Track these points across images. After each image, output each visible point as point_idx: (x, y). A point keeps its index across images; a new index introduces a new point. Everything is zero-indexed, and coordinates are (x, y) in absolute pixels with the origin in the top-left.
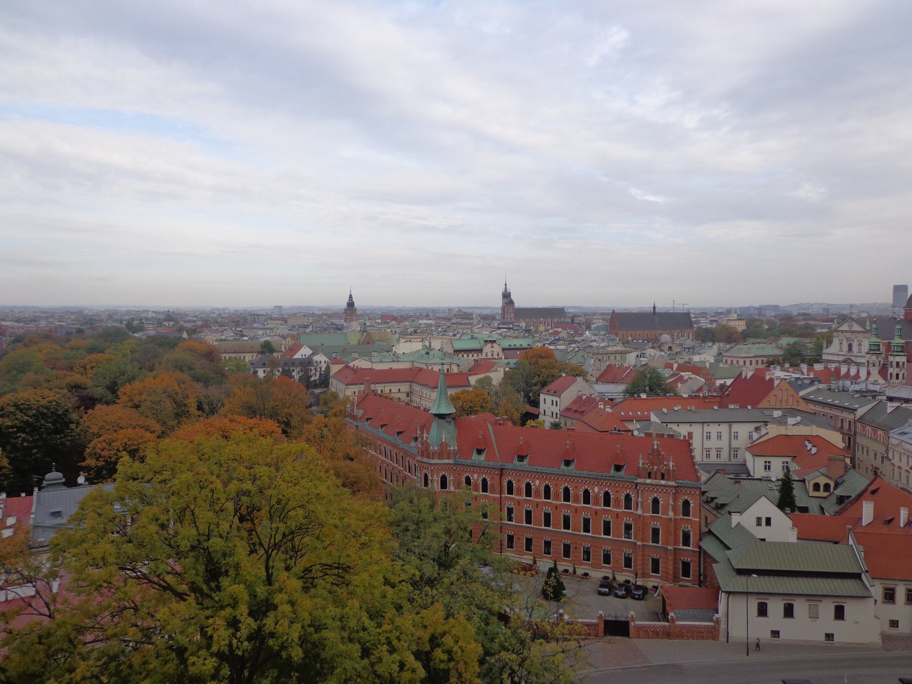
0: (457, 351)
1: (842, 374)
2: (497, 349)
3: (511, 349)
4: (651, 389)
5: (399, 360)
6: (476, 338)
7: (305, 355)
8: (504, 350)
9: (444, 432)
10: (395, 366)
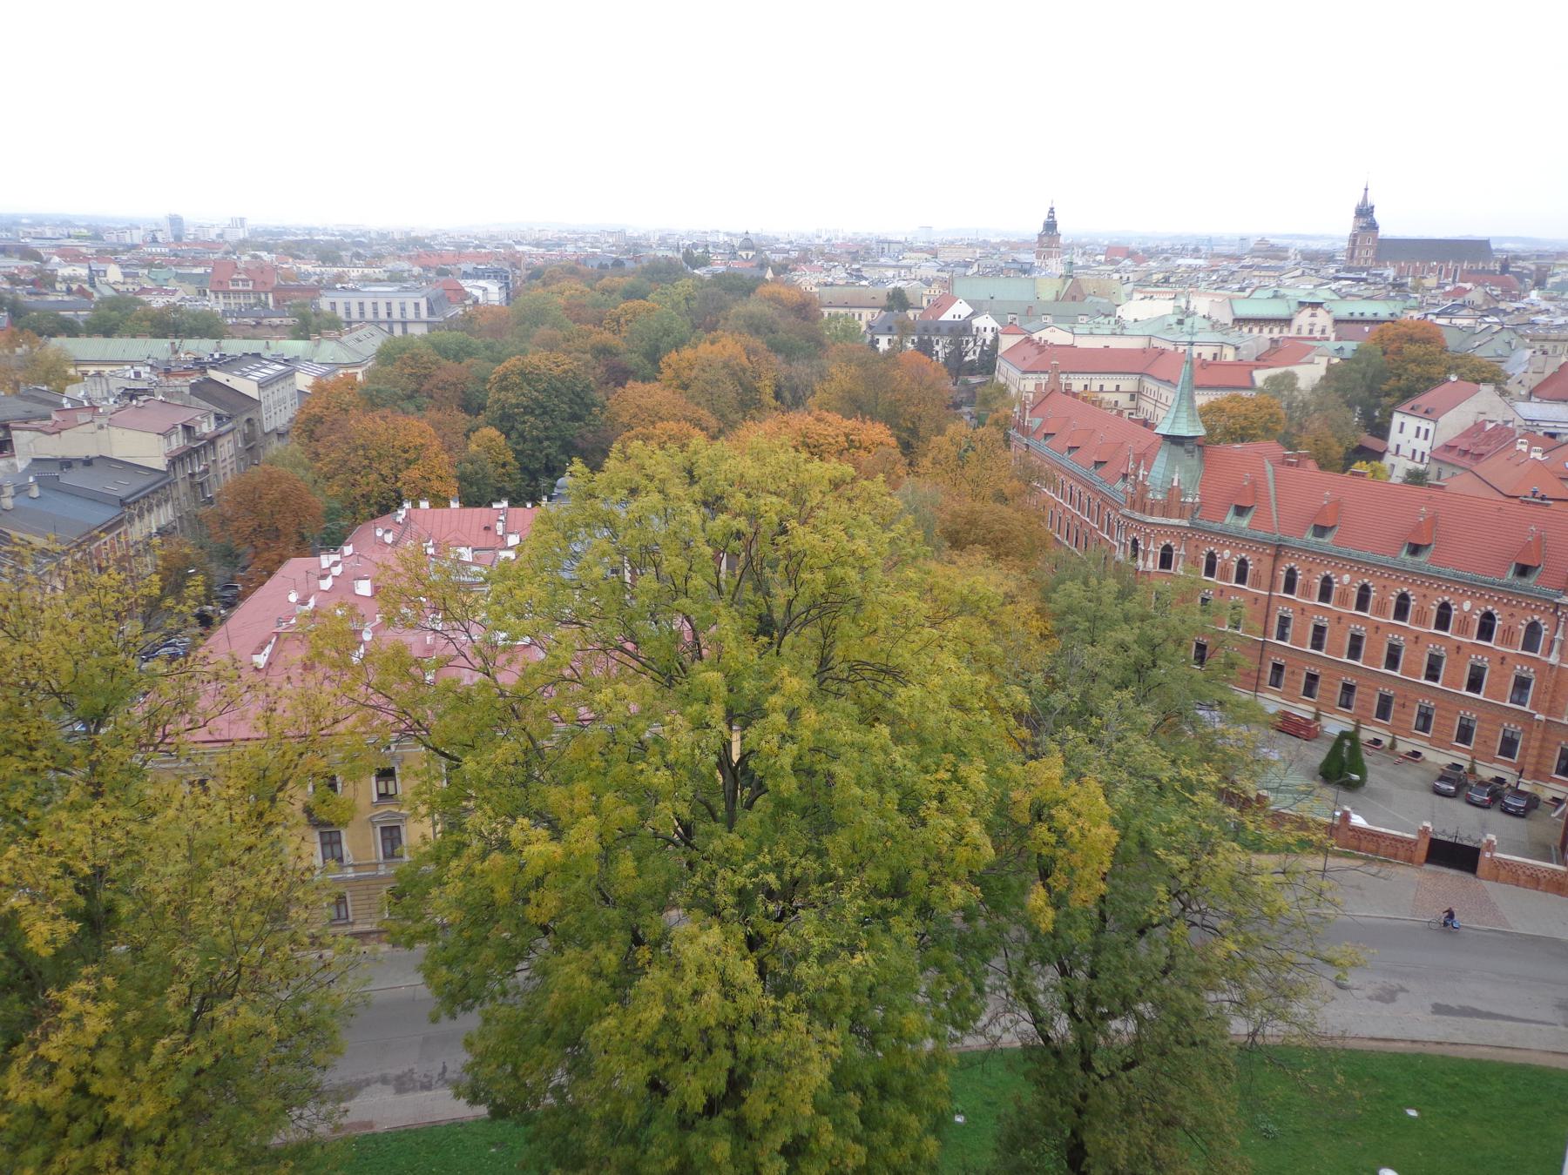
0: (1240, 321)
2: (1323, 319)
3: (1353, 321)
5: (1125, 332)
6: (1283, 297)
8: (1337, 321)
10: (1116, 343)
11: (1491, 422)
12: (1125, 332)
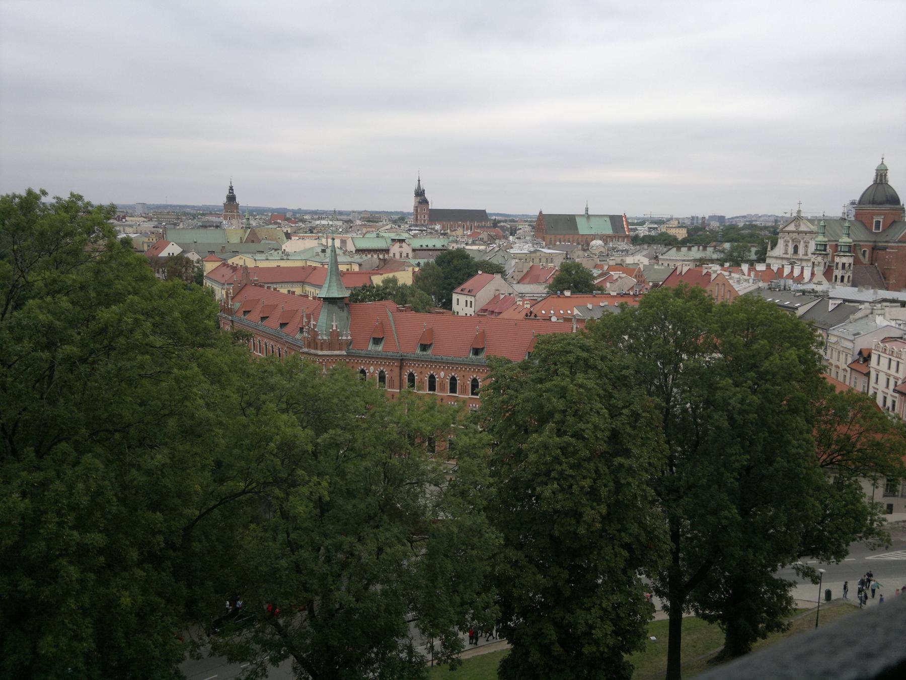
0: (359, 251)
1: (785, 275)
2: (406, 249)
3: (423, 250)
4: (576, 286)
5: (290, 258)
7: (173, 254)
8: (414, 250)
9: (334, 319)
10: (283, 264)
11: (502, 294)
12: (290, 258)
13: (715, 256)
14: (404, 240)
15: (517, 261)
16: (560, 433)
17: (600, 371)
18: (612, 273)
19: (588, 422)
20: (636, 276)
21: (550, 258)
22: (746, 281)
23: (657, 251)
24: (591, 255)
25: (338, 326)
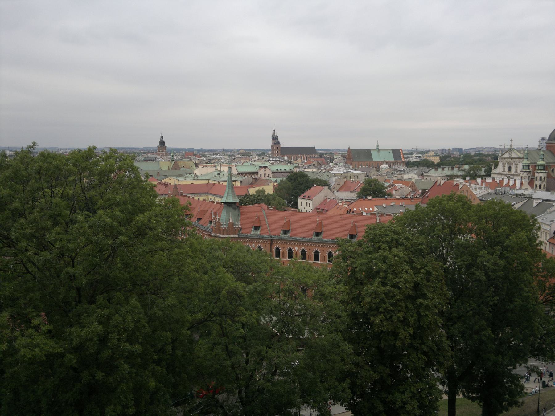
0: (240, 174)
1: (504, 184)
2: (268, 172)
3: (278, 172)
5: (199, 178)
6: (254, 165)
9: (231, 215)
10: (195, 182)
11: (329, 199)
12: (199, 178)
13: (459, 174)
14: (267, 166)
15: (336, 178)
16: (384, 284)
17: (405, 246)
18: (396, 185)
19: (401, 278)
20: (411, 186)
21: (356, 176)
22: (480, 188)
23: (423, 171)
24: (382, 174)
25: (233, 219)
